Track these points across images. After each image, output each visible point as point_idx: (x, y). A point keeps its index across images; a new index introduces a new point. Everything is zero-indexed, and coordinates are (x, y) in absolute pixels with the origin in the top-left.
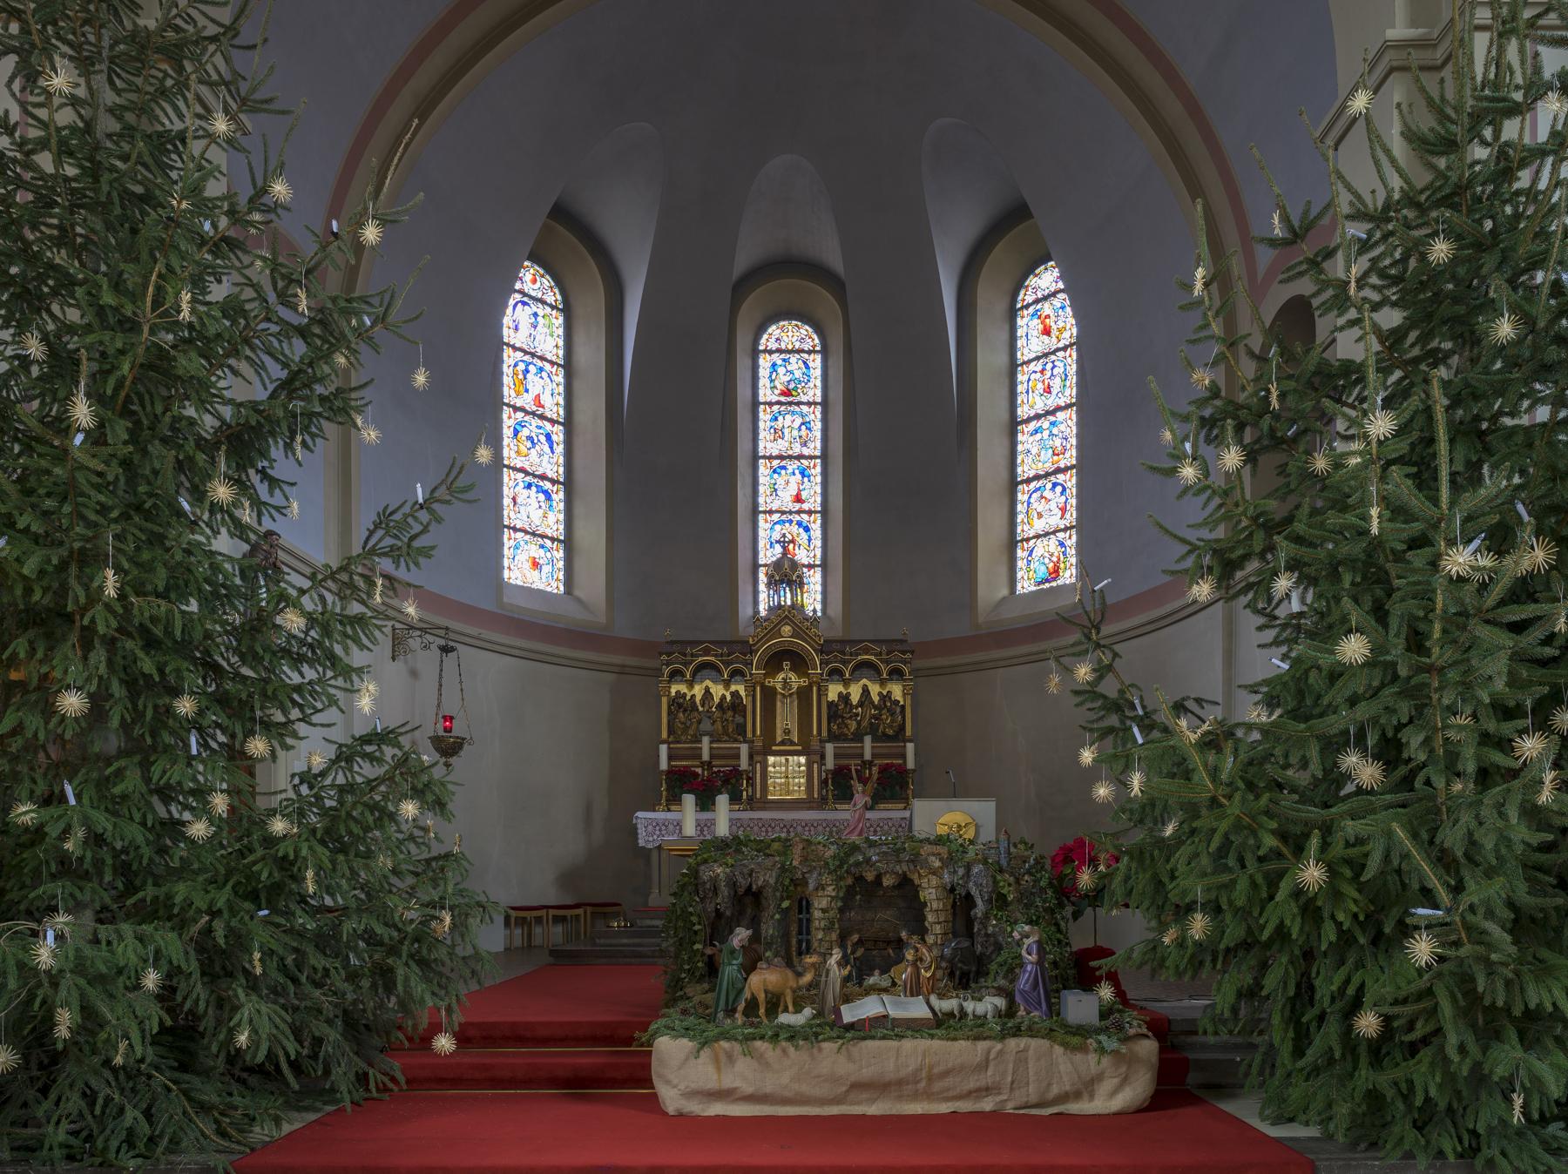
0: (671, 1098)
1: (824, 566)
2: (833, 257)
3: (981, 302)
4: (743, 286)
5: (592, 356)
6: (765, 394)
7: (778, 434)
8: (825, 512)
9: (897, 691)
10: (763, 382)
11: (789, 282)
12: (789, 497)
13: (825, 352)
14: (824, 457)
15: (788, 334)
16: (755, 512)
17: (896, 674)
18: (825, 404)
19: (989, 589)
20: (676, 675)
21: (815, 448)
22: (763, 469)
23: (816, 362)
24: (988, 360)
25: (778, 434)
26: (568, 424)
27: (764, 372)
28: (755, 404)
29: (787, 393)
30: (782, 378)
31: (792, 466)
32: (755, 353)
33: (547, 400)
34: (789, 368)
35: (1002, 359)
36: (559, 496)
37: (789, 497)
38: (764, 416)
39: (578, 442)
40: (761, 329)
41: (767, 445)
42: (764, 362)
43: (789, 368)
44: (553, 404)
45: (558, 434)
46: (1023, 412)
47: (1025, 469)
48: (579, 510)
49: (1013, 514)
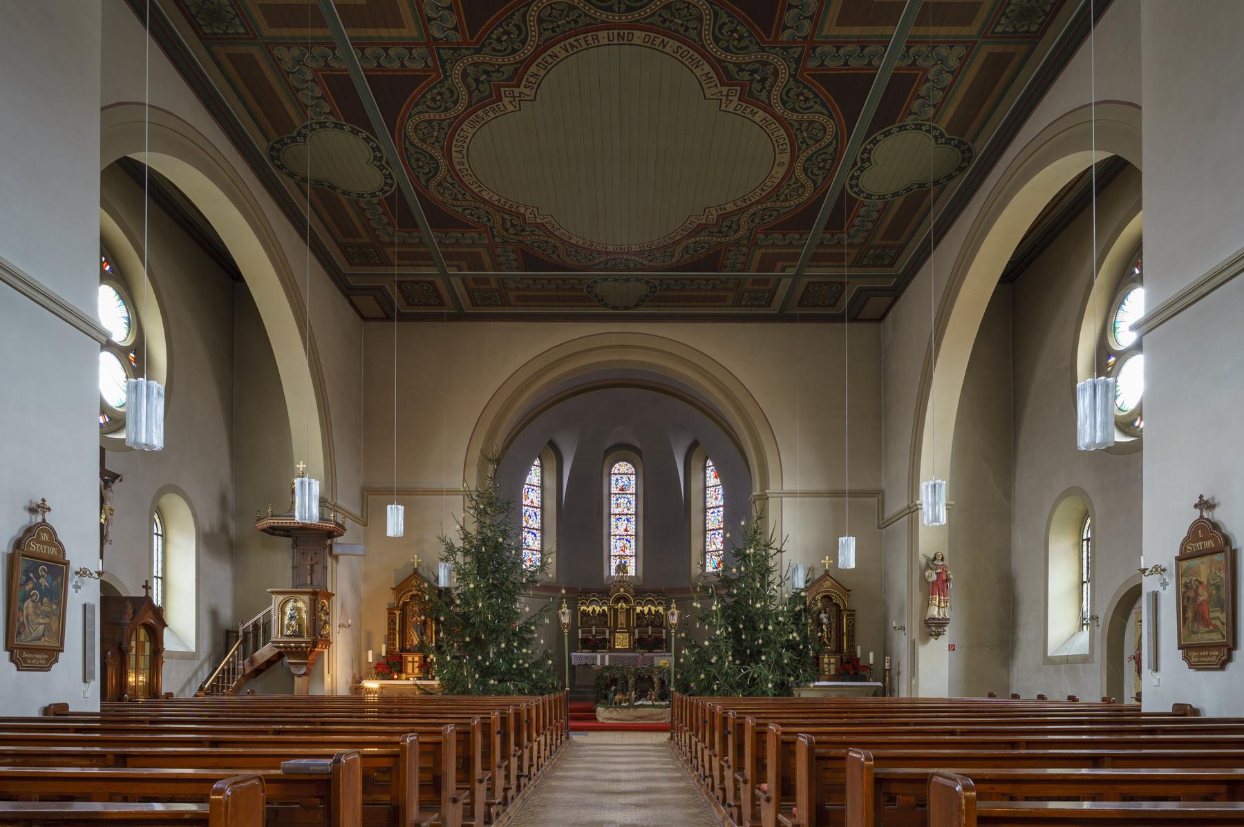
0: (600, 719)
1: (636, 556)
2: (638, 445)
3: (693, 465)
4: (608, 452)
5: (551, 483)
6: (614, 490)
7: (618, 506)
8: (636, 535)
9: (661, 609)
10: (613, 485)
11: (623, 451)
12: (623, 545)
13: (636, 474)
14: (636, 514)
15: (622, 467)
16: (610, 535)
17: (660, 604)
18: (636, 494)
19: (696, 570)
20: (583, 604)
21: (632, 511)
22: (613, 519)
23: (633, 478)
24: (696, 486)
25: (618, 506)
26: (542, 508)
27: (613, 482)
28: (610, 494)
29: (622, 489)
30: (621, 484)
31: (624, 517)
32: (610, 474)
33: (535, 501)
34: (623, 479)
35: (701, 486)
36: (539, 535)
37: (623, 545)
38: (613, 499)
39: (546, 515)
40: (612, 465)
41: (614, 510)
42: (613, 478)
43: (623, 479)
44: (537, 502)
45: (538, 512)
46: (709, 505)
47: (710, 526)
48: (546, 539)
49: (705, 542)
